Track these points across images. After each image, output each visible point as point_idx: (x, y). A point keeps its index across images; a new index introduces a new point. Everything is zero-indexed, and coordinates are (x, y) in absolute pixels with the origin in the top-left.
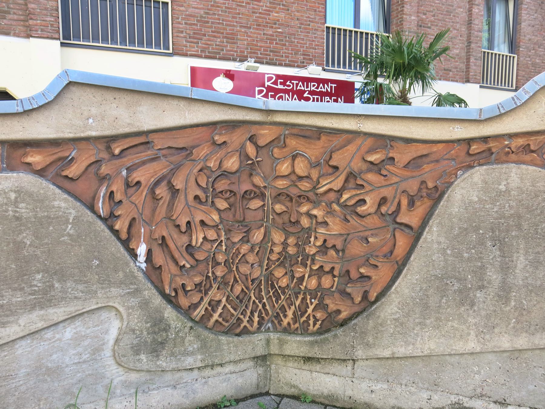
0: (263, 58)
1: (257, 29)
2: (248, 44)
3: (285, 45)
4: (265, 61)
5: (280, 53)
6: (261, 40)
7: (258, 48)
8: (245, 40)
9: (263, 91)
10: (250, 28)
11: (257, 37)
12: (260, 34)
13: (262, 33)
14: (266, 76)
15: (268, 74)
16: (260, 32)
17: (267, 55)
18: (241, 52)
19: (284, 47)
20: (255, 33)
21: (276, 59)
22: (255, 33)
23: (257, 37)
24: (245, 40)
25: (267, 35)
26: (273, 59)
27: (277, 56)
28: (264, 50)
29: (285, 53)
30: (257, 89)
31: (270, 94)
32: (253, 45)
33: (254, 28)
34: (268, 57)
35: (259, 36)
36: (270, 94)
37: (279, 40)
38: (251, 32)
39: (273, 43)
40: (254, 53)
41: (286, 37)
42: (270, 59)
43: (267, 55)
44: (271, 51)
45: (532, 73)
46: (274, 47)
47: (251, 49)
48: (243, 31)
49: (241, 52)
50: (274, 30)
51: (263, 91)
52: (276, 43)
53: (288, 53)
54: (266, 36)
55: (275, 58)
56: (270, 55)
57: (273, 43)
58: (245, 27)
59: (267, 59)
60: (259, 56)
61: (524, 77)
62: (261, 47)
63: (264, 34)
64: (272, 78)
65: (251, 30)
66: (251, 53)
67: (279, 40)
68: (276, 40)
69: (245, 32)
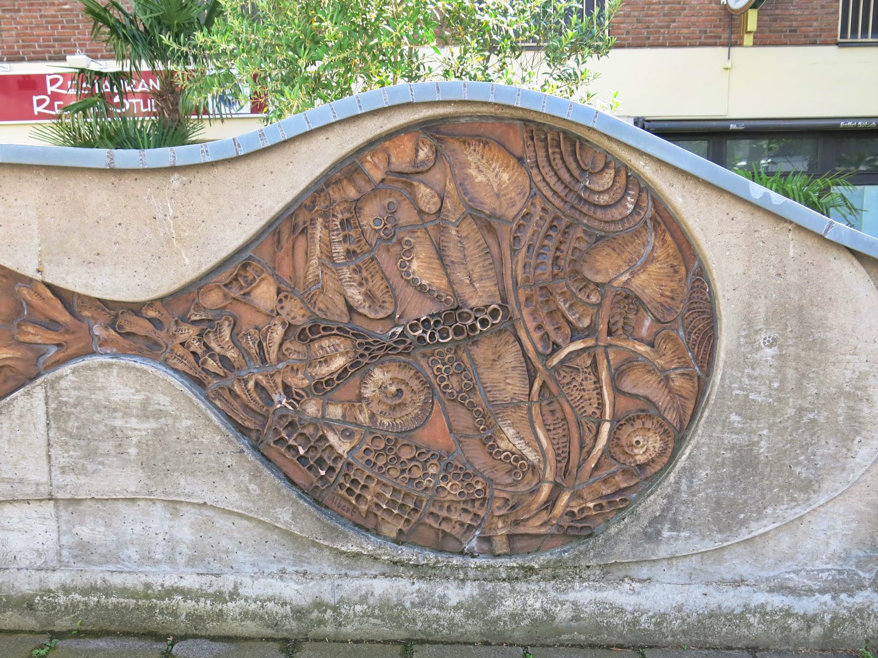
0: (43, 52)
1: (30, 11)
2: (18, 35)
3: (78, 28)
4: (47, 56)
5: (70, 40)
6: (38, 26)
7: (35, 38)
8: (11, 29)
9: (44, 101)
10: (19, 11)
11: (31, 23)
12: (36, 17)
13: (38, 15)
14: (48, 78)
15: (49, 75)
16: (35, 14)
17: (48, 46)
18: (8, 47)
19: (76, 31)
20: (27, 17)
21: (65, 52)
22: (27, 17)
23: (31, 23)
24: (11, 29)
25: (46, 16)
26: (60, 52)
27: (65, 46)
28: (44, 40)
29: (79, 39)
30: (35, 98)
31: (56, 103)
32: (25, 34)
33: (24, 10)
34: (52, 50)
35: (33, 20)
36: (56, 103)
37: (68, 22)
38: (21, 17)
39: (56, 28)
40: (29, 46)
41: (77, 16)
42: (55, 52)
43: (48, 46)
44: (55, 40)
45: (653, 7)
46: (59, 34)
47: (23, 41)
48: (8, 16)
49: (8, 47)
50: (56, 8)
51: (44, 101)
52: (63, 28)
53: (84, 40)
54: (44, 19)
55: (63, 49)
56: (54, 46)
57: (56, 28)
58: (9, 11)
59: (50, 52)
60: (38, 49)
61: (628, 16)
62: (39, 36)
63: (41, 16)
64: (57, 80)
65: (22, 14)
66: (23, 47)
67: (68, 22)
68: (62, 22)
69: (12, 18)
